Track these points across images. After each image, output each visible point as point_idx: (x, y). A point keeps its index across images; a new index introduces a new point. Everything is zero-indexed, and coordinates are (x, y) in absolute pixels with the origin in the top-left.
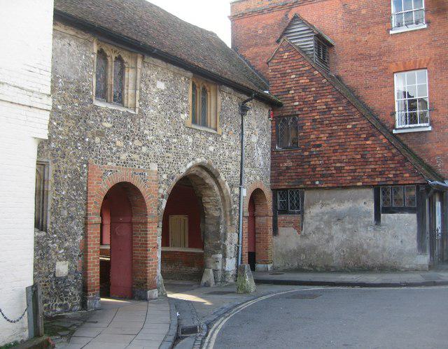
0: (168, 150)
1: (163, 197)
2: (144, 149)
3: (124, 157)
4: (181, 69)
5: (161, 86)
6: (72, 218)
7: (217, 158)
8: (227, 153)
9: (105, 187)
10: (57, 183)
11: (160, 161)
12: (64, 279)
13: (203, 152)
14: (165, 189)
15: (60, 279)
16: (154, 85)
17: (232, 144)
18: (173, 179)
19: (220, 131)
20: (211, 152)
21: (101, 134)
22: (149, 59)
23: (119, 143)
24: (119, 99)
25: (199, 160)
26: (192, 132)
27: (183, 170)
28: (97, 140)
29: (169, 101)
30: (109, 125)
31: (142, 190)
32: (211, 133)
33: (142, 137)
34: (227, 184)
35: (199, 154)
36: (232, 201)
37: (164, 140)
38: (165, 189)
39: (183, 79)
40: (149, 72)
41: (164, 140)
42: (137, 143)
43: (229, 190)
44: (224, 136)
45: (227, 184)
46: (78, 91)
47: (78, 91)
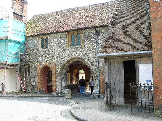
0: (59, 56)
1: (59, 69)
2: (51, 57)
3: (45, 60)
4: (62, 33)
5: (56, 40)
6: (35, 74)
7: (82, 54)
8: (88, 52)
9: (41, 67)
10: (31, 68)
11: (57, 59)
12: (34, 86)
13: (74, 54)
14: (59, 67)
15: (33, 86)
16: (54, 41)
17: (91, 48)
18: (62, 63)
19: (83, 45)
20: (79, 53)
21: (40, 56)
22: (51, 35)
23: (44, 57)
24: (47, 47)
25: (72, 57)
26: (69, 49)
27: (65, 61)
28: (39, 58)
29: (60, 44)
30: (41, 54)
31: (50, 67)
32: (78, 47)
33: (51, 54)
34: (88, 62)
35: (72, 55)
36: (93, 68)
37: (58, 54)
38: (59, 67)
39: (64, 35)
40: (52, 38)
41: (58, 54)
42: (49, 56)
43: (91, 65)
44: (86, 47)
45: (88, 62)
46: (35, 49)
47: (35, 49)
